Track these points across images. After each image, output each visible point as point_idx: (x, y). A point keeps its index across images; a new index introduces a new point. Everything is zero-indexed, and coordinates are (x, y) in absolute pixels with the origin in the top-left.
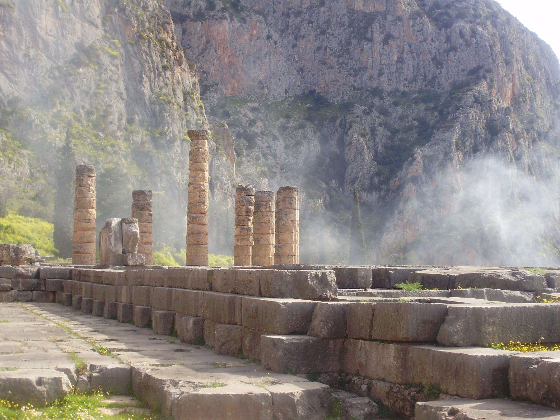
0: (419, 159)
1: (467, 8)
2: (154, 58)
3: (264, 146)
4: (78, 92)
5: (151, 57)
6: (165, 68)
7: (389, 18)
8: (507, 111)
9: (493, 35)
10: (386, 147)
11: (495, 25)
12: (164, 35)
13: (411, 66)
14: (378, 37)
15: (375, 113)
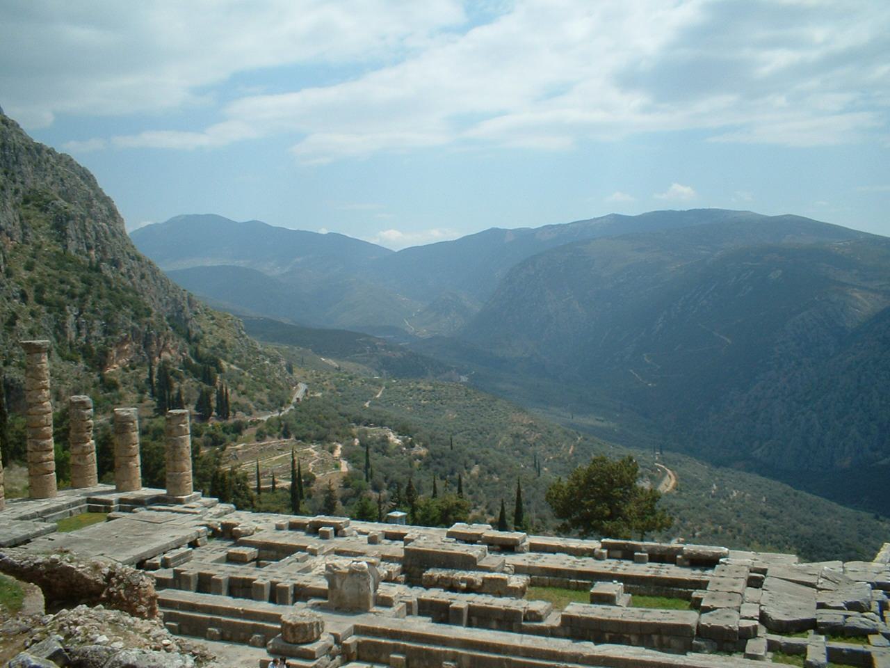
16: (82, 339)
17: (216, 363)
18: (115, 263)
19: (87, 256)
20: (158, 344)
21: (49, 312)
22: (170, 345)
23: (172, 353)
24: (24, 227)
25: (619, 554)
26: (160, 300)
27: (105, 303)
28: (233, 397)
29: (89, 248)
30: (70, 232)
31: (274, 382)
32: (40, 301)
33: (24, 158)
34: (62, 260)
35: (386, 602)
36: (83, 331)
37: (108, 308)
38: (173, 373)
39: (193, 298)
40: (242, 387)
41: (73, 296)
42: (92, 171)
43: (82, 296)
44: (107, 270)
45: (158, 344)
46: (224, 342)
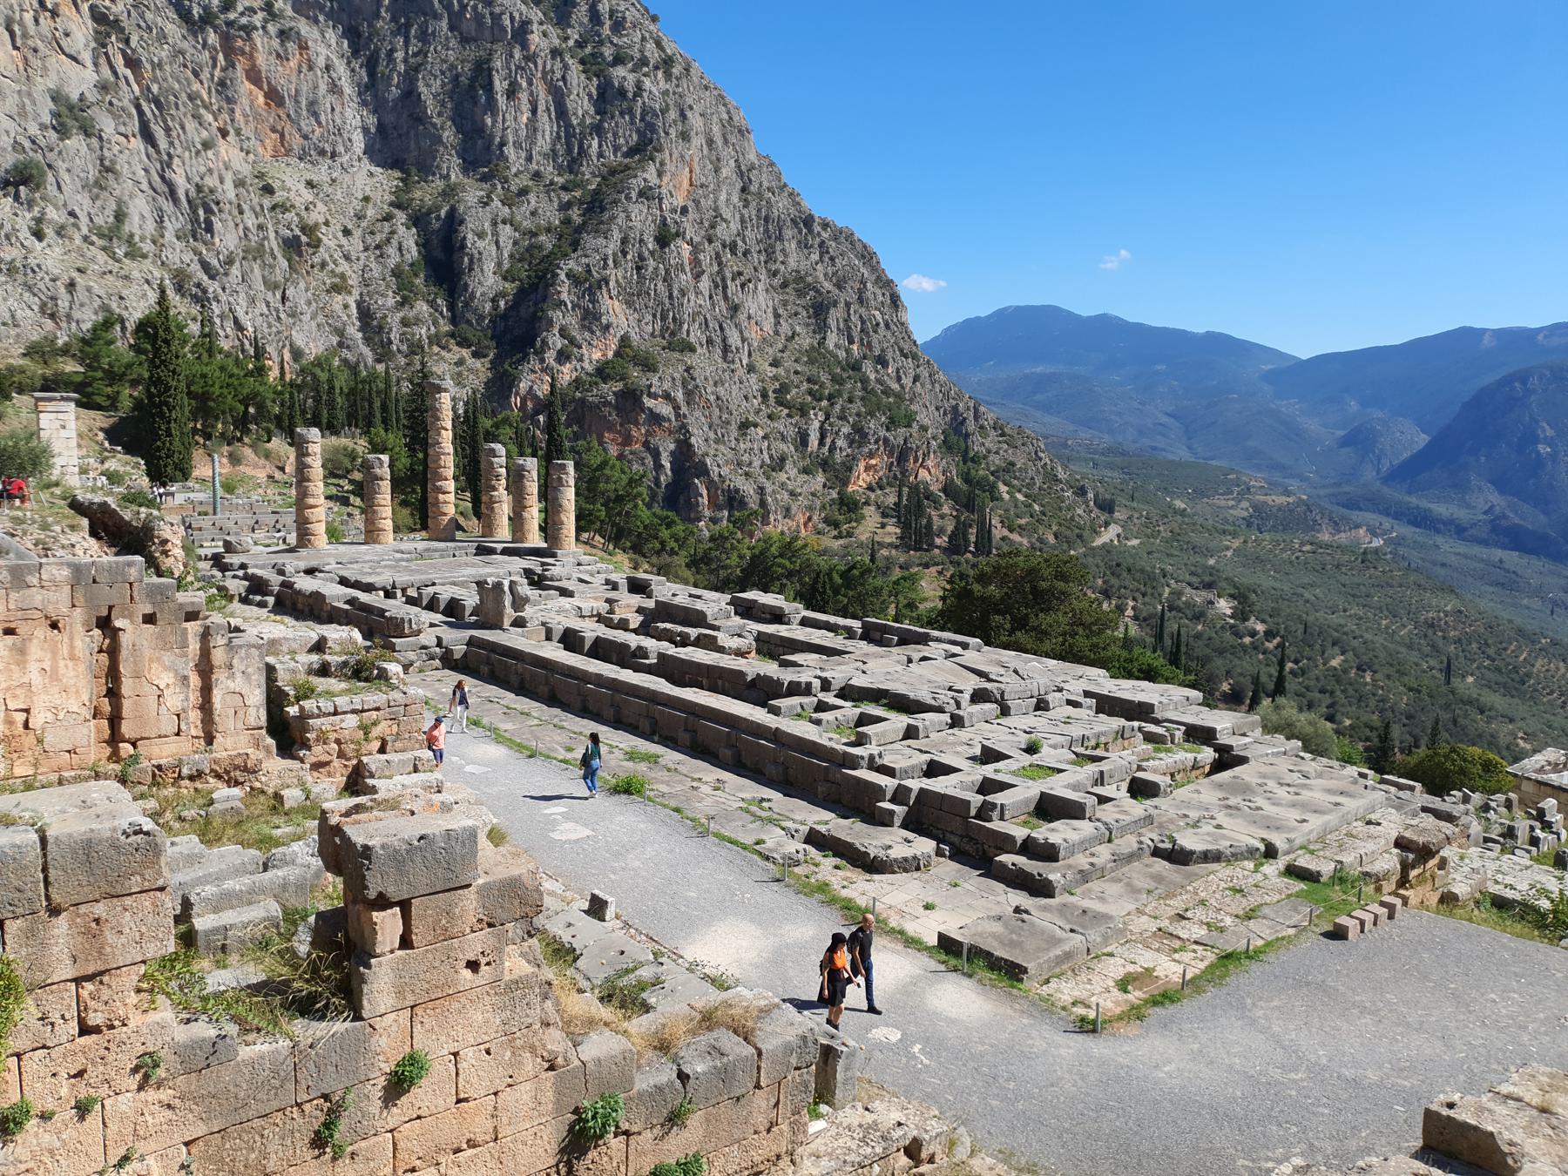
0: (563, 277)
1: (630, 47)
2: (188, 126)
3: (332, 244)
4: (66, 177)
5: (183, 128)
6: (207, 145)
7: (517, 54)
8: (684, 210)
9: (666, 93)
10: (511, 256)
11: (668, 76)
12: (196, 86)
13: (548, 133)
14: (500, 85)
15: (496, 203)
16: (825, 450)
17: (992, 491)
18: (882, 361)
19: (848, 351)
20: (916, 461)
21: (789, 416)
22: (930, 463)
23: (932, 473)
24: (777, 316)
25: (877, 635)
26: (937, 409)
27: (857, 406)
28: (998, 532)
29: (851, 342)
30: (832, 323)
31: (1072, 519)
32: (780, 402)
33: (788, 233)
34: (816, 355)
35: (519, 623)
36: (828, 441)
37: (858, 415)
38: (929, 496)
39: (982, 409)
40: (1023, 522)
41: (820, 400)
42: (874, 246)
43: (830, 398)
44: (868, 368)
45: (916, 461)
46: (1012, 464)
